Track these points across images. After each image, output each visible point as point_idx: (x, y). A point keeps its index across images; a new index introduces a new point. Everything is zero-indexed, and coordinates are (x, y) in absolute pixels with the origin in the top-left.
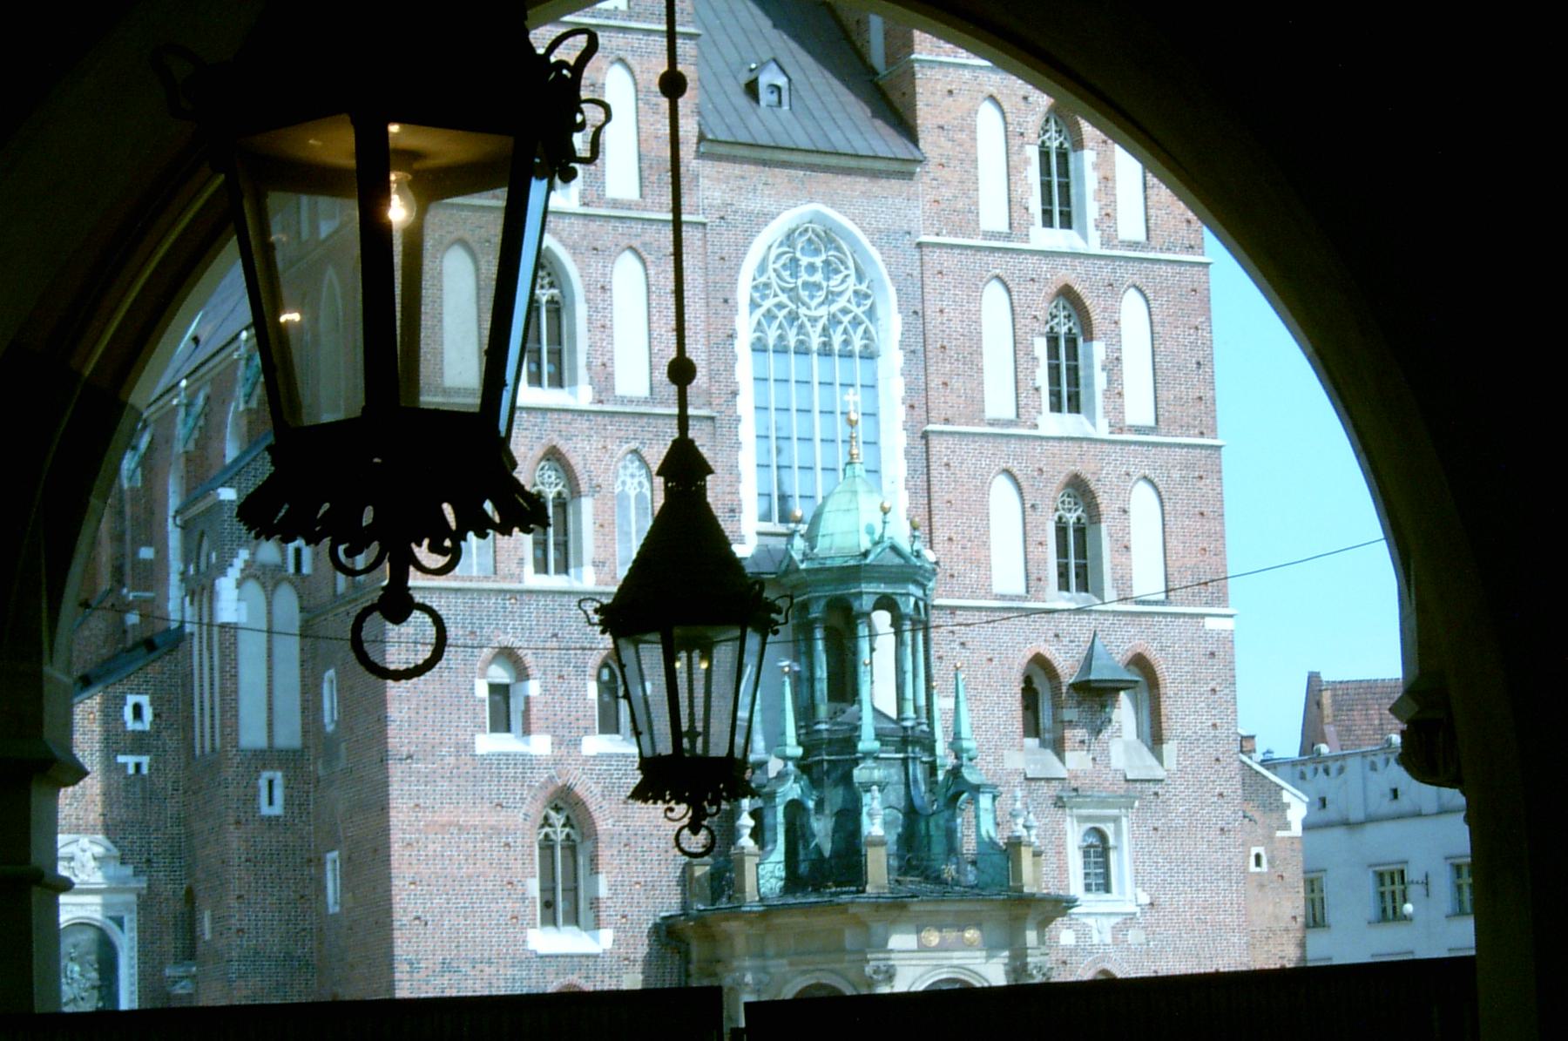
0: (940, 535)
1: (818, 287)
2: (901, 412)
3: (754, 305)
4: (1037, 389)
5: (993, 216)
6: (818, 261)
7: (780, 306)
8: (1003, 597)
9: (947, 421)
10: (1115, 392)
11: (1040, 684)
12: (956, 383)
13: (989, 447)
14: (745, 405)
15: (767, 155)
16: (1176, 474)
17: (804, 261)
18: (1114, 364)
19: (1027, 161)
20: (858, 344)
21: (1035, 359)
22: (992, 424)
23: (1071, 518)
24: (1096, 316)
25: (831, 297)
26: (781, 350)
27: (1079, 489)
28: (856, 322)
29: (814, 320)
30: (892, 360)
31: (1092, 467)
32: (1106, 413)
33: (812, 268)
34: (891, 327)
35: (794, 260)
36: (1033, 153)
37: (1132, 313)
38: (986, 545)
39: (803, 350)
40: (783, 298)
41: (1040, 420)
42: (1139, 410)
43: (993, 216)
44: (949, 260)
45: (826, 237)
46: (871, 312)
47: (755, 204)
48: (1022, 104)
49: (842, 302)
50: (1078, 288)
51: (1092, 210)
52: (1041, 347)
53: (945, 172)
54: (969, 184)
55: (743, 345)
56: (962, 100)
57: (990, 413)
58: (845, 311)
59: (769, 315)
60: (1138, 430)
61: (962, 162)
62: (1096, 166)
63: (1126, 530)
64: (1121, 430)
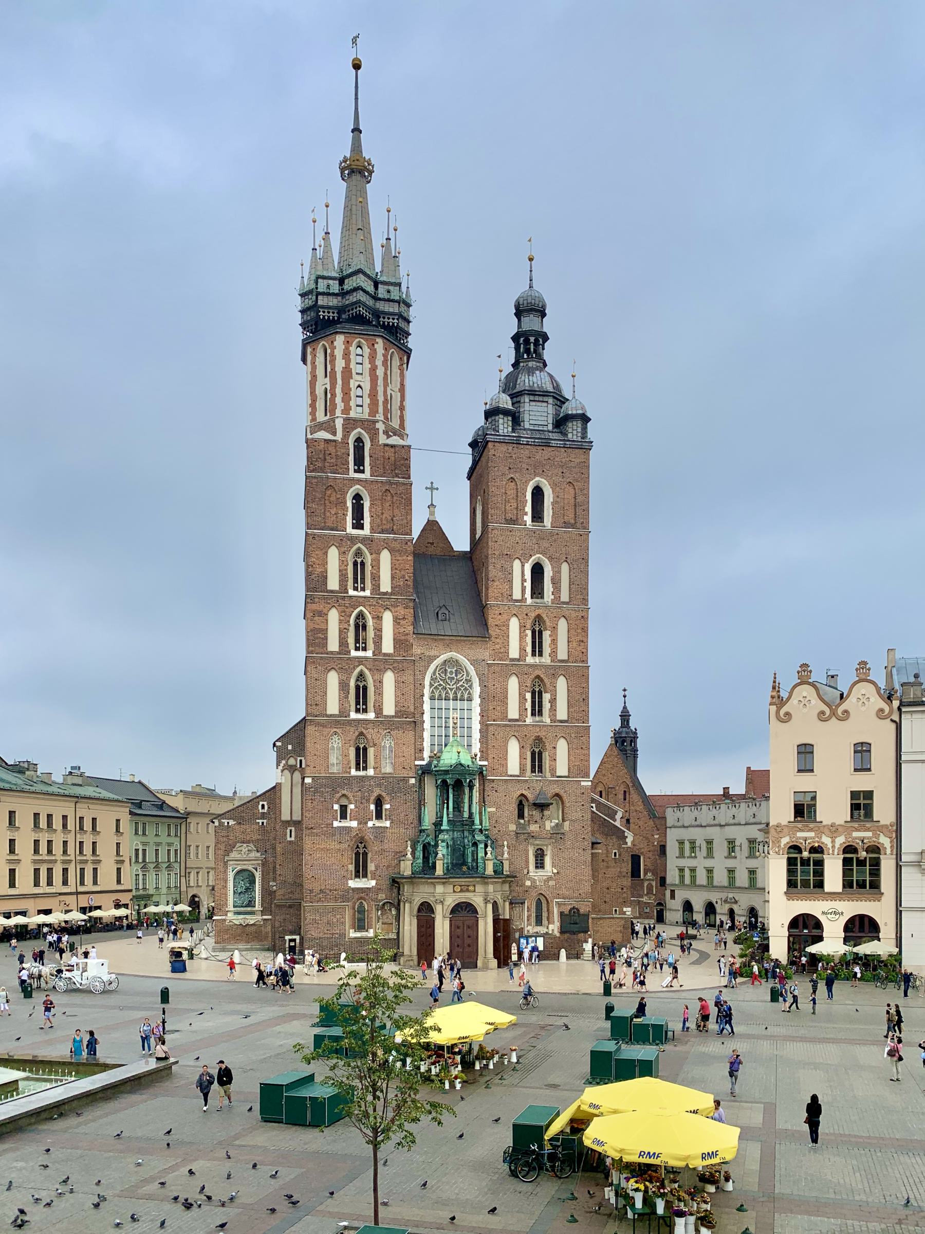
0: (491, 756)
1: (453, 678)
2: (479, 718)
3: (431, 685)
4: (526, 709)
5: (514, 653)
6: (454, 670)
7: (440, 685)
8: (511, 776)
9: (494, 721)
10: (553, 709)
11: (525, 803)
12: (498, 708)
13: (508, 729)
14: (427, 717)
15: (436, 637)
16: (573, 735)
17: (449, 670)
18: (553, 701)
19: (526, 635)
20: (466, 696)
21: (526, 700)
22: (510, 720)
23: (537, 750)
24: (548, 685)
25: (458, 681)
26: (440, 699)
27: (539, 740)
28: (466, 689)
29: (451, 689)
30: (477, 701)
31: (544, 734)
32: (550, 716)
33: (451, 673)
34: (477, 690)
35: (446, 670)
36: (529, 633)
37: (562, 684)
38: (506, 759)
39: (447, 699)
40: (442, 683)
41: (527, 720)
42: (562, 714)
43: (514, 653)
44: (497, 669)
45: (457, 663)
46: (471, 686)
47: (432, 653)
48: (525, 617)
49: (461, 683)
50: (542, 676)
51: (547, 649)
52: (528, 696)
53: (498, 640)
54: (506, 645)
55: (426, 698)
56: (505, 616)
57: (510, 717)
58: (462, 686)
59: (436, 688)
60: (561, 721)
61: (503, 636)
62: (550, 636)
63: (555, 754)
64: (555, 722)
